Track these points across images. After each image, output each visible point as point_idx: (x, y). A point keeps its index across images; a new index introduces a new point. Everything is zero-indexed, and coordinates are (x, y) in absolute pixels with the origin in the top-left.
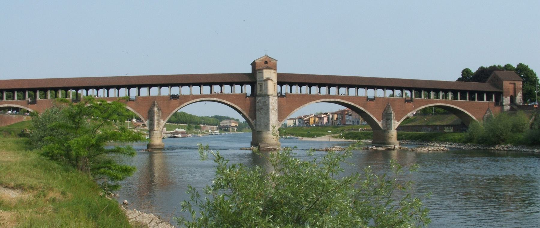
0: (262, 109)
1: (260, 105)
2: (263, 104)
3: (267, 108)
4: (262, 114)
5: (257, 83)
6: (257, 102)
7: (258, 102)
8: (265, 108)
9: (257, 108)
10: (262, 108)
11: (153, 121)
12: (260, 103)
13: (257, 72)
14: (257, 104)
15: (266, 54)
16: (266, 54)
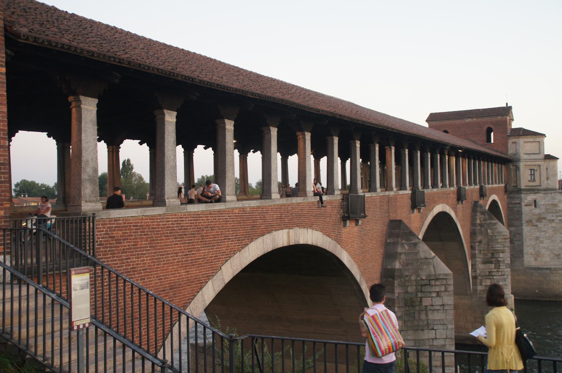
0: (544, 221)
1: (537, 211)
2: (547, 209)
3: (560, 218)
4: (545, 231)
5: (522, 165)
6: (523, 204)
7: (526, 205)
8: (552, 218)
9: (525, 218)
10: (545, 218)
11: (498, 266)
12: (535, 206)
13: (510, 141)
14: (525, 209)
15: (507, 104)
16: (507, 104)
